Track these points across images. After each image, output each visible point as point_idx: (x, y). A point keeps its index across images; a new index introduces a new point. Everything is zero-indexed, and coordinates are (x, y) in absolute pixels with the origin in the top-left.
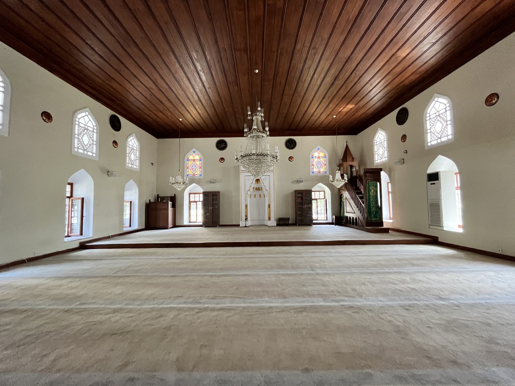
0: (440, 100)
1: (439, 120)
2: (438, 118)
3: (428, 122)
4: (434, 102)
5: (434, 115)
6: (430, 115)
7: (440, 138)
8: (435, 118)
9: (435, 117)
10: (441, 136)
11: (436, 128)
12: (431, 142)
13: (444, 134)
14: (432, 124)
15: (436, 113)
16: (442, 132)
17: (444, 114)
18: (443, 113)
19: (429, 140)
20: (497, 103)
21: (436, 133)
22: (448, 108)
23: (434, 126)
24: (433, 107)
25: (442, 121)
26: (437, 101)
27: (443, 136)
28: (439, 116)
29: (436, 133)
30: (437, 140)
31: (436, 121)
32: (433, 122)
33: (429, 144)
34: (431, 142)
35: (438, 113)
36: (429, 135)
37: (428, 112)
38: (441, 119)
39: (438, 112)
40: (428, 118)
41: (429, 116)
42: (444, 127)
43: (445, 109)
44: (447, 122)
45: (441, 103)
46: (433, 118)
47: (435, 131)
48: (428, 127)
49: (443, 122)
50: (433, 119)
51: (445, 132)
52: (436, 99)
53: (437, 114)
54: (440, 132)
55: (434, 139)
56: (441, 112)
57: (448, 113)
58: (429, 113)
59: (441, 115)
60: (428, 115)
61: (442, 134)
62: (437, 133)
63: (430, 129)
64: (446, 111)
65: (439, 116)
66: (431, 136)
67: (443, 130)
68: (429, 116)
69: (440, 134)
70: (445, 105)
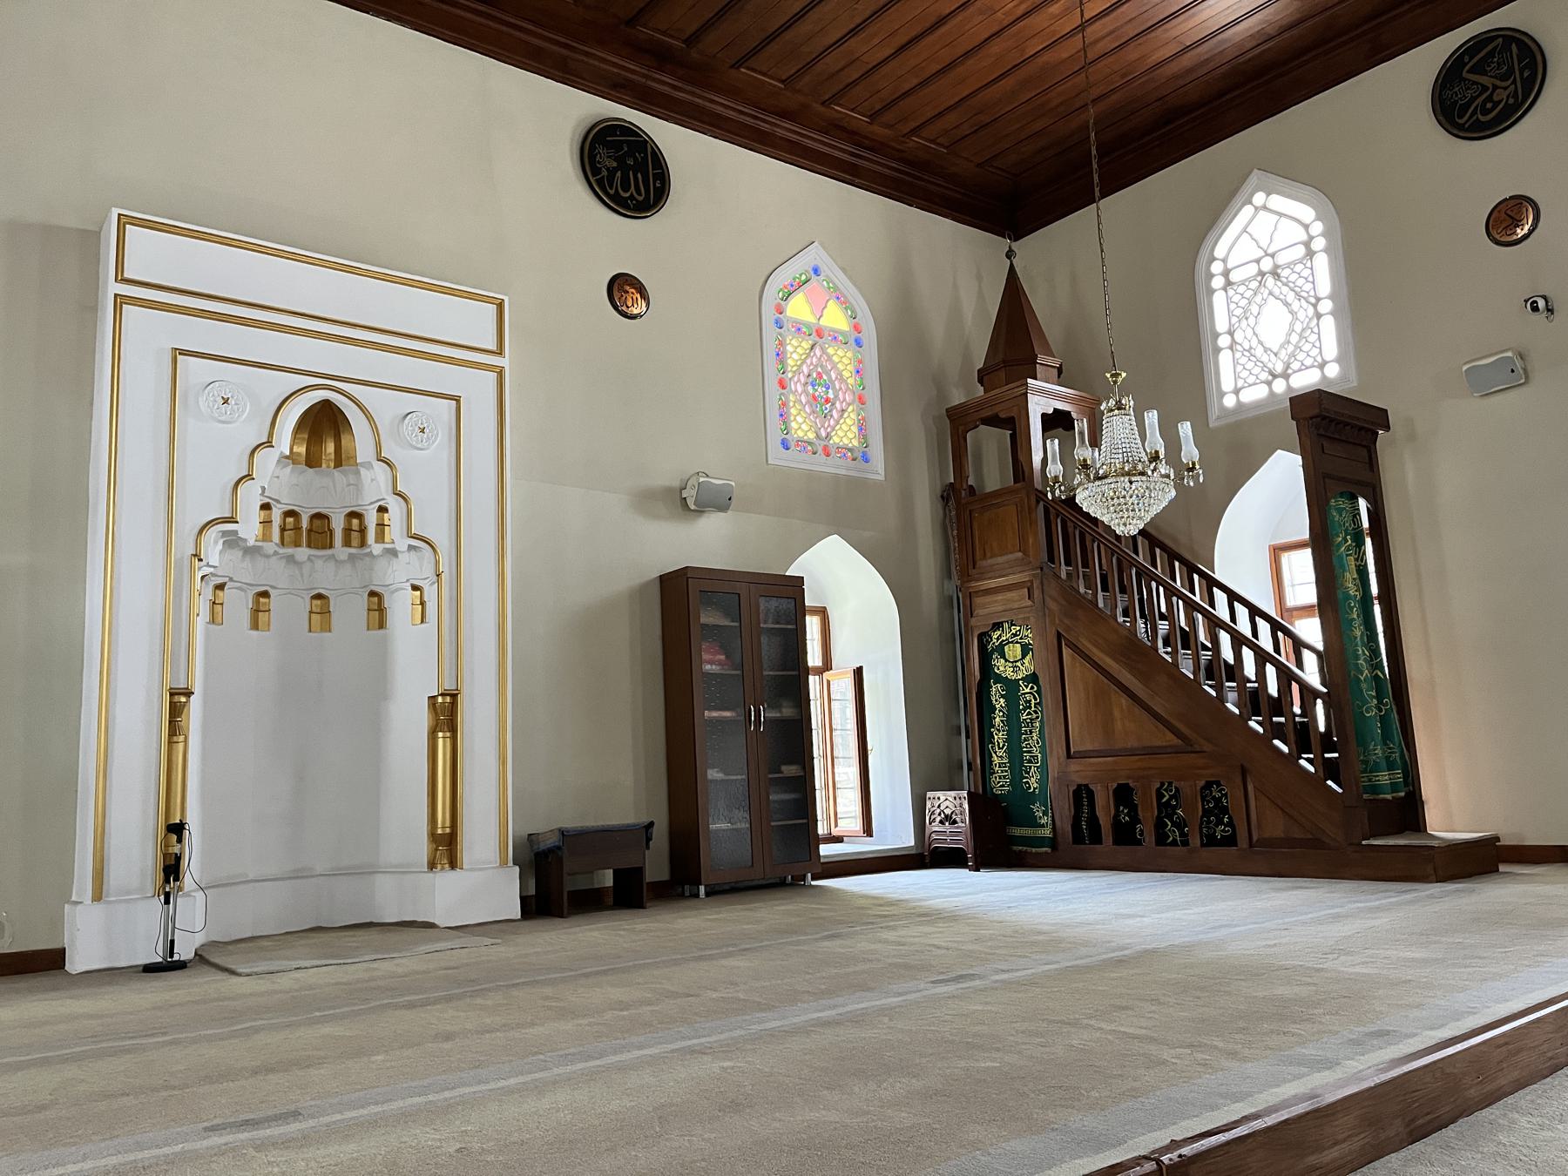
0: (1278, 202)
1: (1276, 291)
2: (1270, 281)
3: (1219, 300)
4: (1247, 211)
5: (1253, 269)
6: (1229, 266)
8: (1254, 285)
9: (1254, 278)
10: (1288, 367)
11: (1257, 330)
12: (1237, 391)
13: (1301, 356)
14: (1238, 312)
15: (1258, 261)
16: (1291, 348)
17: (1299, 267)
18: (1294, 263)
19: (1227, 383)
20: (1530, 239)
21: (1259, 351)
22: (1319, 244)
23: (1252, 320)
24: (1245, 230)
25: (1291, 297)
26: (1265, 208)
27: (1295, 366)
28: (1275, 274)
29: (1259, 351)
30: (1269, 383)
31: (1258, 299)
32: (1243, 303)
33: (1229, 401)
34: (1237, 391)
35: (1269, 258)
36: (1225, 359)
37: (1220, 251)
38: (1285, 289)
40: (1217, 282)
41: (1226, 273)
43: (1307, 244)
44: (1315, 306)
45: (1281, 215)
46: (1243, 283)
47: (1254, 343)
48: (1221, 324)
49: (1296, 306)
50: (1242, 289)
51: (1307, 347)
52: (1259, 198)
53: (1267, 264)
54: (1282, 346)
55: (1251, 379)
56: (1282, 259)
57: (1322, 262)
58: (1224, 261)
59: (1284, 273)
60: (1216, 268)
61: (1293, 355)
62: (1266, 350)
63: (1231, 333)
64: (1310, 254)
66: (1235, 363)
67: (1294, 338)
68: (1226, 273)
69: (1283, 355)
70: (1306, 227)
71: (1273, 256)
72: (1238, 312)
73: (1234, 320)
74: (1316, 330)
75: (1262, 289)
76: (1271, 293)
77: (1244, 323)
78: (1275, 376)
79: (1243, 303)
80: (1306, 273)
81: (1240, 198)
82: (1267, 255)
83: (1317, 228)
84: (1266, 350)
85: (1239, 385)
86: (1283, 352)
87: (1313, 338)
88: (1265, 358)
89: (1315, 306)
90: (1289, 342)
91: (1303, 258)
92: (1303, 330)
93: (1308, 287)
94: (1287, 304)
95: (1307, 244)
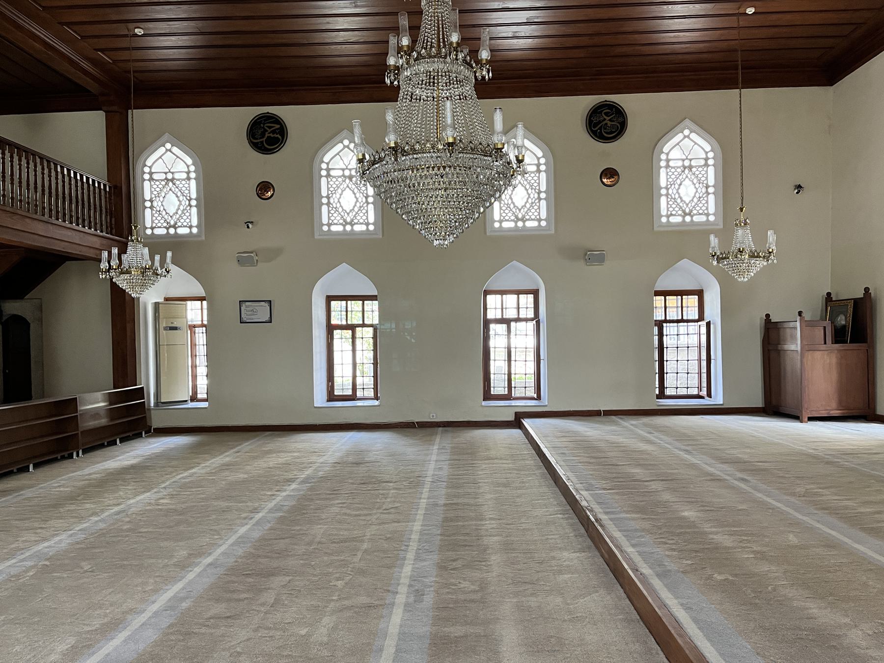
5: (163, 176)
6: (153, 171)
7: (175, 227)
14: (155, 193)
25: (179, 194)
26: (170, 150)
31: (165, 190)
38: (177, 190)
39: (173, 173)
42: (182, 208)
44: (189, 201)
49: (181, 198)
55: (159, 225)
56: (177, 176)
64: (189, 178)
65: (172, 180)
66: (153, 215)
67: (180, 212)
71: (173, 173)
72: (155, 193)
73: (153, 196)
74: (189, 211)
75: (167, 186)
76: (170, 190)
77: (158, 199)
78: (170, 227)
79: (158, 189)
80: (187, 185)
81: (159, 142)
82: (170, 172)
83: (192, 168)
84: (167, 213)
85: (154, 225)
86: (175, 217)
87: (188, 214)
88: (166, 217)
89: (189, 201)
90: (177, 213)
91: (186, 179)
92: (183, 210)
93: (187, 192)
94: (177, 196)
95: (188, 173)
